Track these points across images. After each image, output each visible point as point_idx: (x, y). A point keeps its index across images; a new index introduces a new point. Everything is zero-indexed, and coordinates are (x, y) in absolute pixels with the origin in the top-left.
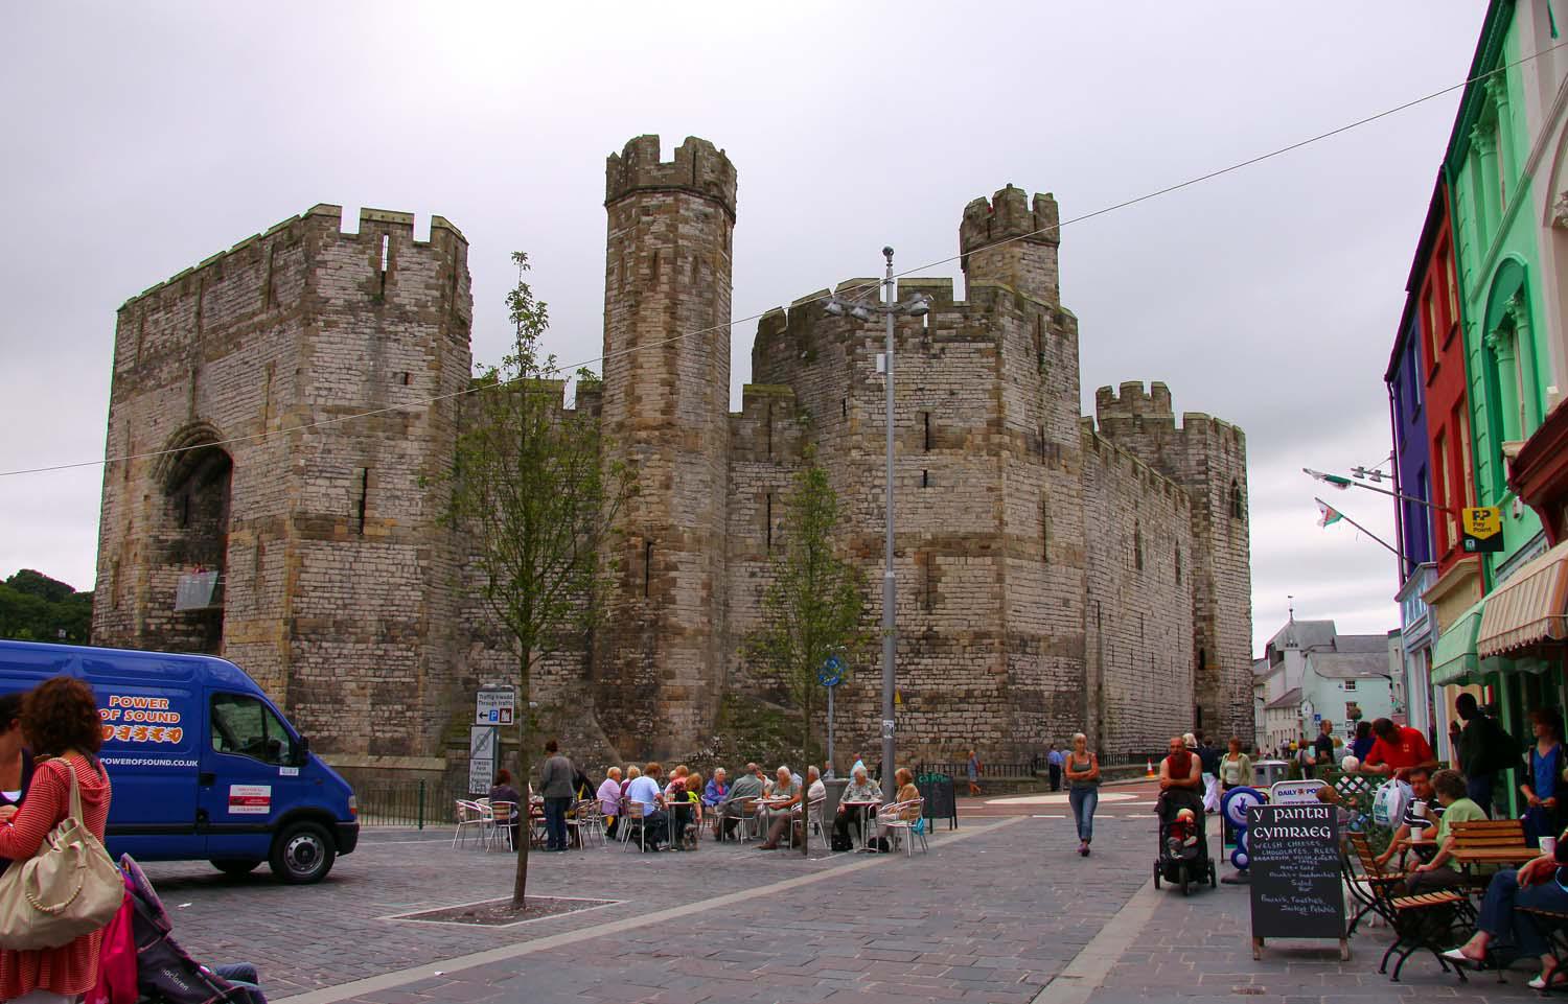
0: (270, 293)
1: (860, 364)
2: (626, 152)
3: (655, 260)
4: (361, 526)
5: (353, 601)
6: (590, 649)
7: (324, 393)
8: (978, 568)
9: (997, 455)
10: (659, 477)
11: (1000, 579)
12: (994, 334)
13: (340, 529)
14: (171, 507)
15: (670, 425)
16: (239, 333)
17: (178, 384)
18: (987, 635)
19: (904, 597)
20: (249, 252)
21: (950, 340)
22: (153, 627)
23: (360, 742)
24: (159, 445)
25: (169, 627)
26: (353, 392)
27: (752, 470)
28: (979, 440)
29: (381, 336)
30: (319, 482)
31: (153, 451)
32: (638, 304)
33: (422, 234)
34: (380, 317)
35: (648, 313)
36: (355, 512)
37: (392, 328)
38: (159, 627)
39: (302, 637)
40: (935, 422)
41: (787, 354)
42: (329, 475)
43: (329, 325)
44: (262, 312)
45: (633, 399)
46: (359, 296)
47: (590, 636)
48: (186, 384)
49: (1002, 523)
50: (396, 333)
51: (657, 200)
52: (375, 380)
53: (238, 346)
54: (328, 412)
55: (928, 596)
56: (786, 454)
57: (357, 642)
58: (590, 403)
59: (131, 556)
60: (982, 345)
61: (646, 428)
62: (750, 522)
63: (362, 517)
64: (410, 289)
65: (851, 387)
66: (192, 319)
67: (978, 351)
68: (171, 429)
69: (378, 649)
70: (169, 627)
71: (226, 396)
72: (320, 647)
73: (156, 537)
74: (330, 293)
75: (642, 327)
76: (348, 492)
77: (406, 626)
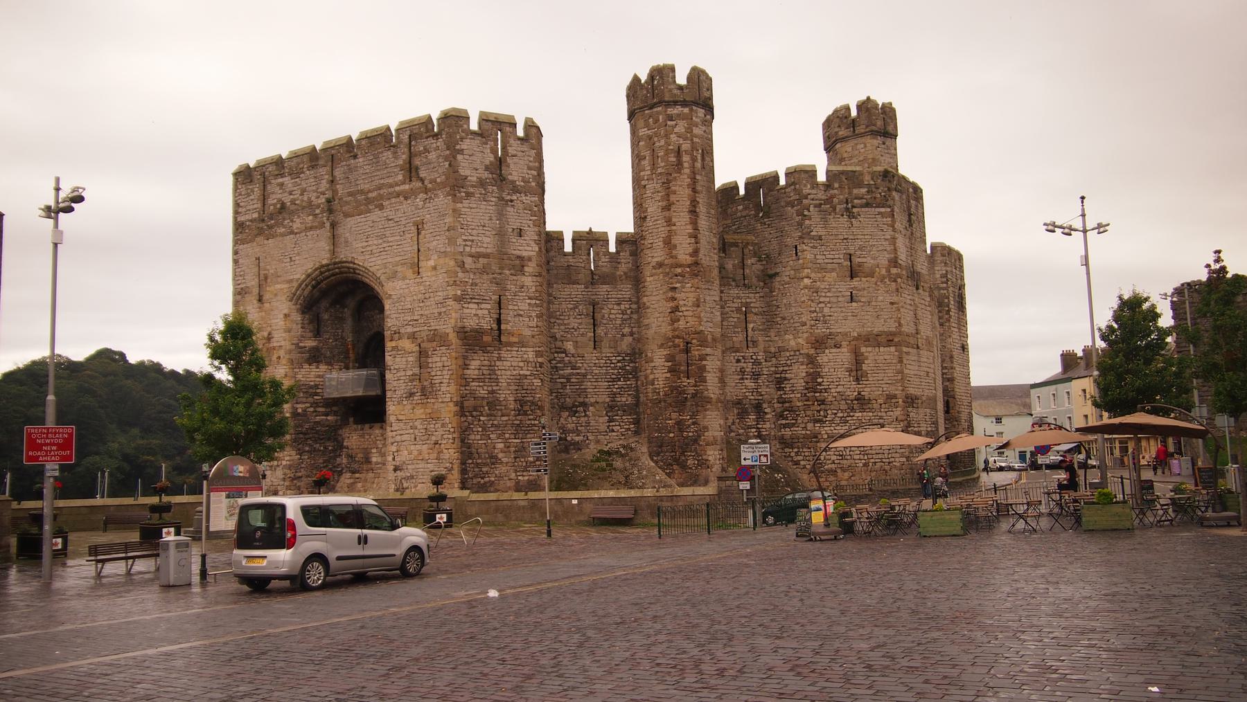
0: (411, 171)
1: (807, 222)
2: (652, 76)
3: (678, 153)
6: (638, 414)
8: (888, 353)
9: (895, 281)
10: (692, 297)
11: (901, 361)
12: (890, 202)
13: (487, 339)
15: (696, 263)
16: (381, 197)
18: (895, 397)
19: (842, 373)
20: (379, 139)
21: (862, 206)
23: (509, 484)
26: (488, 243)
27: (734, 292)
28: (884, 272)
29: (504, 203)
30: (471, 306)
31: (291, 281)
32: (669, 182)
33: (520, 132)
34: (501, 189)
35: (676, 188)
36: (495, 326)
38: (305, 410)
40: (856, 260)
41: (744, 213)
43: (469, 195)
44: (404, 183)
45: (668, 243)
46: (486, 175)
47: (637, 404)
48: (326, 232)
49: (900, 325)
51: (677, 110)
52: (501, 234)
53: (381, 207)
55: (857, 371)
56: (754, 280)
58: (628, 248)
59: (274, 358)
60: (882, 210)
61: (680, 266)
62: (735, 327)
63: (499, 329)
64: (516, 171)
65: (801, 237)
66: (324, 185)
67: (880, 213)
68: (309, 266)
75: (673, 198)
77: (533, 403)
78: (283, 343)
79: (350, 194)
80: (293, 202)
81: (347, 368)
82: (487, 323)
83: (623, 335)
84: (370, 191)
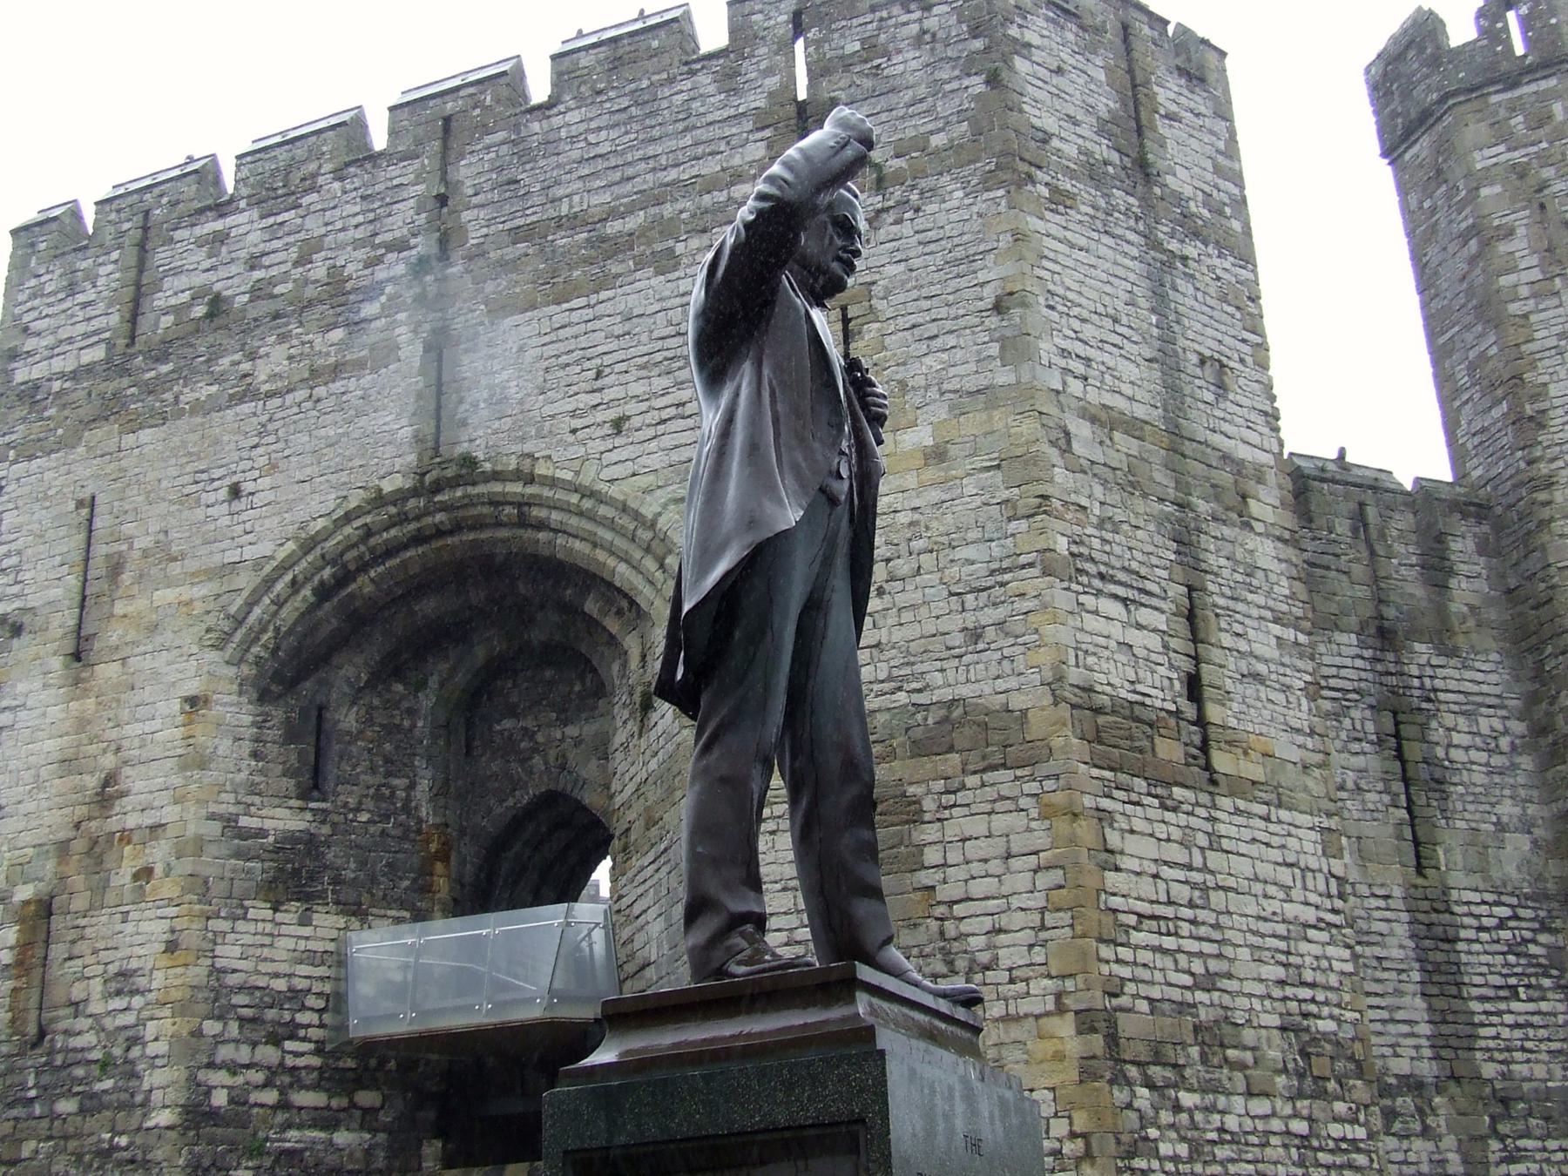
4: (1205, 747)
5: (1222, 966)
7: (1078, 366)
14: (273, 734)
16: (668, 229)
17: (337, 386)
22: (220, 1099)
24: (265, 548)
25: (270, 1097)
37: (1174, 246)
38: (238, 1099)
39: (1133, 1071)
42: (1121, 591)
46: (1102, 150)
50: (1184, 259)
52: (1166, 358)
54: (1093, 420)
57: (1250, 1094)
59: (123, 877)
63: (1201, 722)
69: (1296, 1115)
70: (270, 1097)
71: (609, 395)
72: (1177, 1108)
73: (229, 822)
74: (1049, 123)
76: (1166, 646)
78: (170, 814)
79: (517, 235)
80: (258, 292)
81: (420, 916)
82: (1161, 688)
83: (1501, 827)
84: (612, 214)
